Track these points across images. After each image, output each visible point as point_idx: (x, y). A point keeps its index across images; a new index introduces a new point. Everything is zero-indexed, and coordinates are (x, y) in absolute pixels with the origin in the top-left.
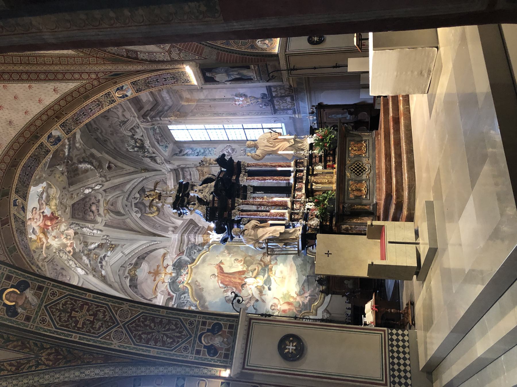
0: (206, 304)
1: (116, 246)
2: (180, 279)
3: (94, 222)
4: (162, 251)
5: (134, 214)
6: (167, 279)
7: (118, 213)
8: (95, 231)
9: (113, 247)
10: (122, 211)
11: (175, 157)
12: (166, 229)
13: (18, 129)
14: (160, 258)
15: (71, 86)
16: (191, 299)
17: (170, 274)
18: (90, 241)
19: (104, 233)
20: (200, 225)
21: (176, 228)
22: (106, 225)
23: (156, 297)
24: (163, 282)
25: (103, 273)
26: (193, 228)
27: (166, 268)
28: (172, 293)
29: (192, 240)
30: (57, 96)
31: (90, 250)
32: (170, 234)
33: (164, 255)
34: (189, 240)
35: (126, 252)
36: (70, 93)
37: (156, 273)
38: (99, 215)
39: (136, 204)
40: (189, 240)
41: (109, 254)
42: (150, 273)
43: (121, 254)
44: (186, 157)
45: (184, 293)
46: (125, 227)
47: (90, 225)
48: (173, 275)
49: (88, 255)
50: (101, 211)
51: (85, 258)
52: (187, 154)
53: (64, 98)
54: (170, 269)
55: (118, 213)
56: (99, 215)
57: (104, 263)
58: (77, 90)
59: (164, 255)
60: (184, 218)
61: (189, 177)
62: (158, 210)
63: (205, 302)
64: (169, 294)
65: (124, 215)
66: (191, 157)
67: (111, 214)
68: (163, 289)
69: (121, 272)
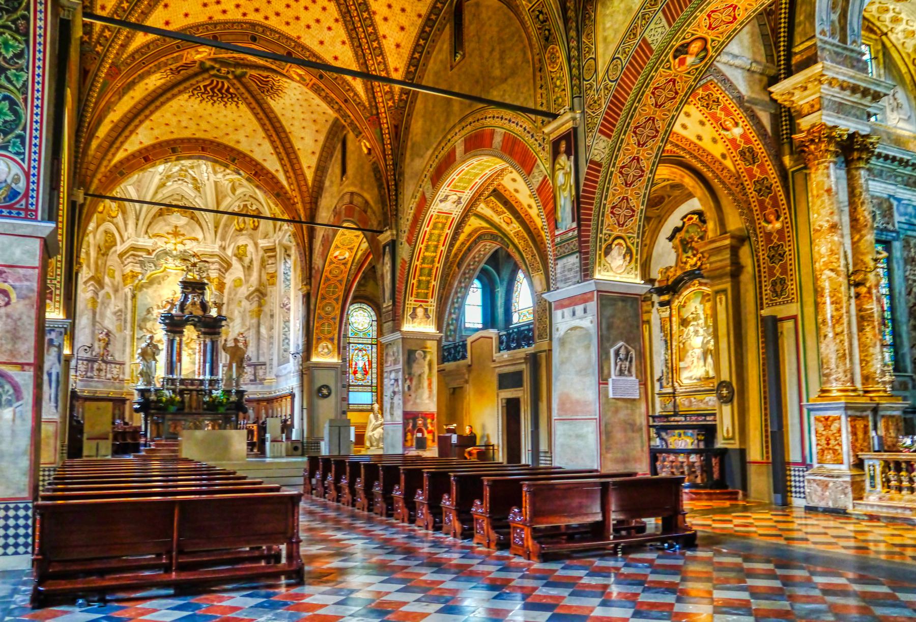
0: (145, 290)
1: (199, 191)
2: (170, 260)
3: (215, 172)
4: (200, 236)
5: (237, 204)
6: (170, 247)
7: (234, 189)
8: (205, 175)
9: (197, 189)
10: (237, 192)
11: (283, 250)
12: (223, 238)
13: (236, 147)
14: (193, 235)
15: (284, 182)
16: (149, 273)
17: (175, 249)
18: (195, 170)
19: (207, 182)
20: (227, 274)
21: (224, 249)
22: (216, 183)
23: (150, 237)
24: (166, 243)
25: (169, 184)
26: (224, 267)
27: (182, 243)
28: (154, 253)
29: (213, 267)
30: (273, 172)
31: (186, 171)
32: (218, 242)
33: (196, 239)
34: (213, 263)
35: (197, 200)
36: (278, 182)
37: (176, 234)
38: (224, 176)
39: (245, 206)
40: (213, 263)
41: (190, 185)
42: (176, 227)
43: (193, 195)
44: (283, 261)
45: (155, 266)
46: (220, 198)
47: (210, 170)
48: (174, 253)
49: (181, 170)
50: (228, 177)
51: (177, 168)
52: (286, 262)
53: (273, 177)
54: (180, 247)
55: (234, 189)
56: (224, 176)
57: (180, 182)
58: (282, 187)
59: (196, 239)
60: (234, 258)
61: (270, 262)
62: (241, 230)
63: (147, 288)
64: (153, 251)
65: (234, 194)
66: (283, 267)
67: (230, 185)
68: (159, 244)
69: (176, 197)
